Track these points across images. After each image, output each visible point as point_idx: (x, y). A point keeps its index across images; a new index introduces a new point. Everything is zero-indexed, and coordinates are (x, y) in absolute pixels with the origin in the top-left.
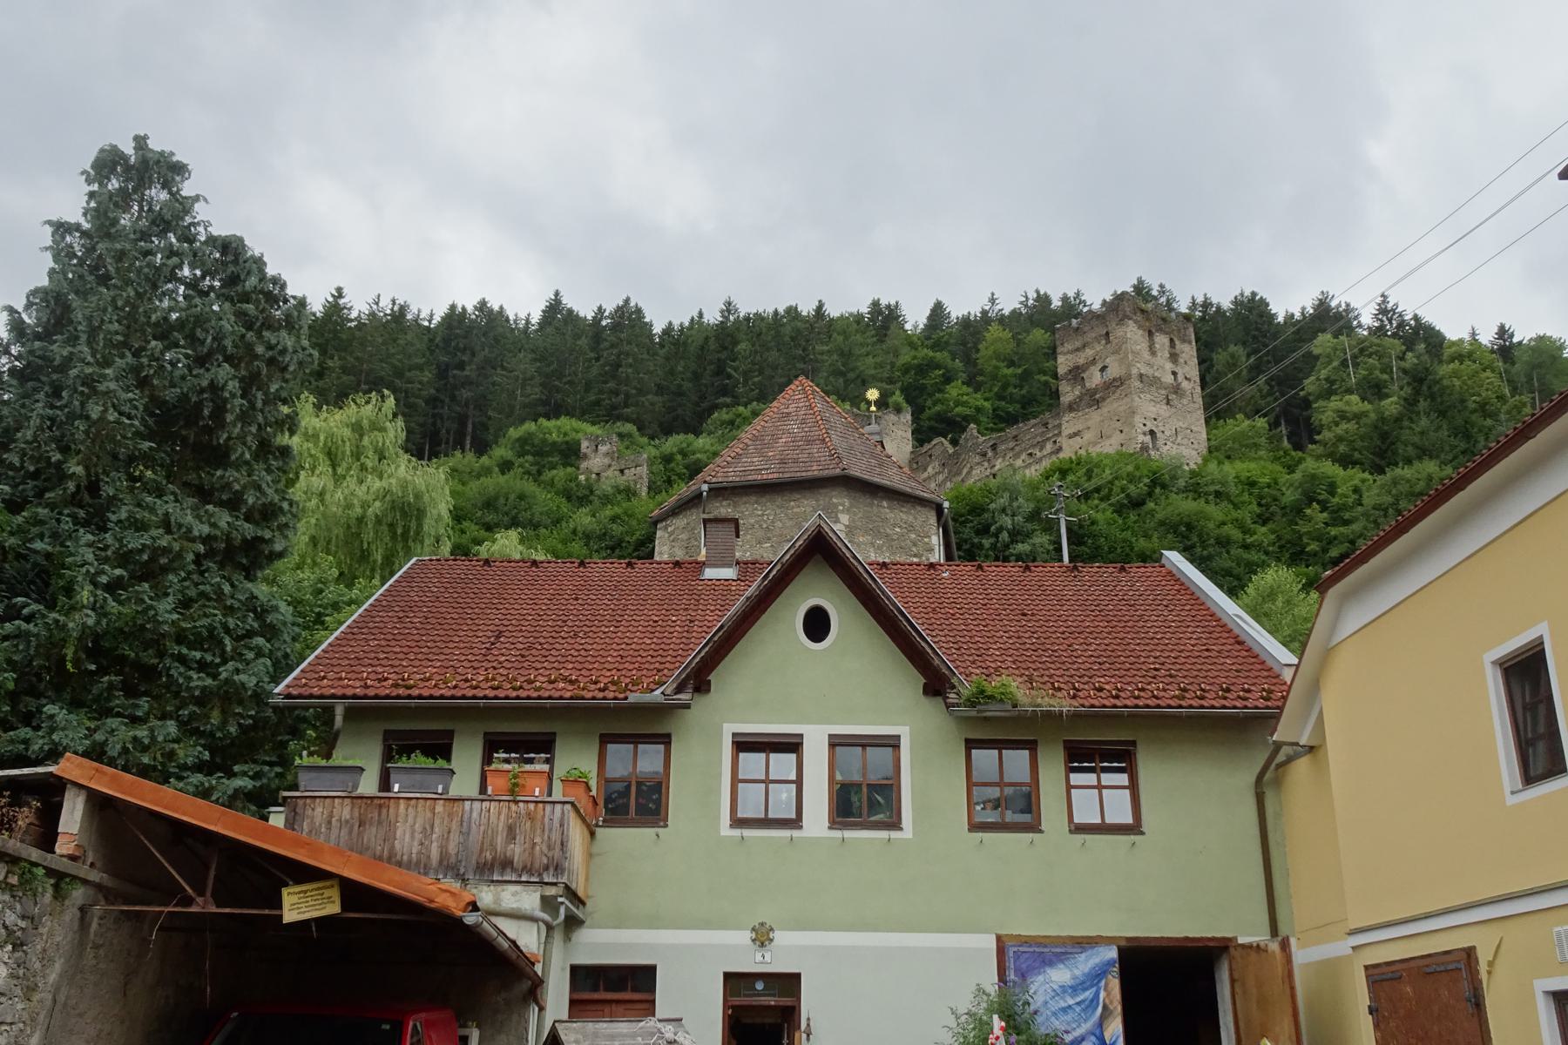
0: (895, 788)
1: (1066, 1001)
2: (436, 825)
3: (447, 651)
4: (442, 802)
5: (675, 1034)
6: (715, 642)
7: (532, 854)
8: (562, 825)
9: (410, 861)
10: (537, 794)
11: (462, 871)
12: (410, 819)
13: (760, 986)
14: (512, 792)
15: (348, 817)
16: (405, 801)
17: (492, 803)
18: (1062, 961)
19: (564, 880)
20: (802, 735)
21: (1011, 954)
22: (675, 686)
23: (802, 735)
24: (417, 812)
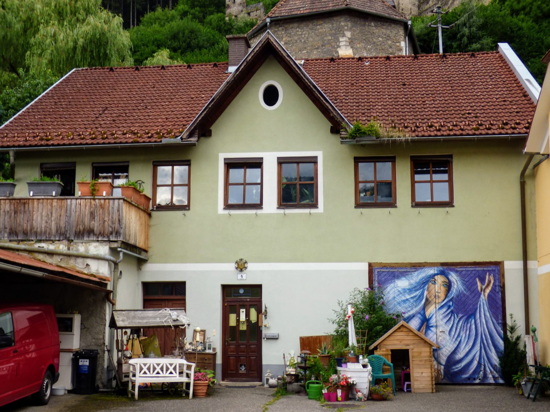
0: (315, 185)
1: (405, 297)
2: (53, 212)
3: (75, 119)
4: (56, 200)
5: (178, 316)
6: (210, 108)
7: (103, 226)
8: (118, 211)
9: (41, 232)
10: (104, 194)
11: (68, 236)
12: (40, 210)
13: (241, 291)
14: (93, 195)
15: (8, 209)
16: (37, 200)
17: (82, 200)
18: (404, 276)
19: (121, 239)
20: (262, 158)
21: (376, 273)
22: (188, 133)
23: (262, 158)
24: (43, 206)
